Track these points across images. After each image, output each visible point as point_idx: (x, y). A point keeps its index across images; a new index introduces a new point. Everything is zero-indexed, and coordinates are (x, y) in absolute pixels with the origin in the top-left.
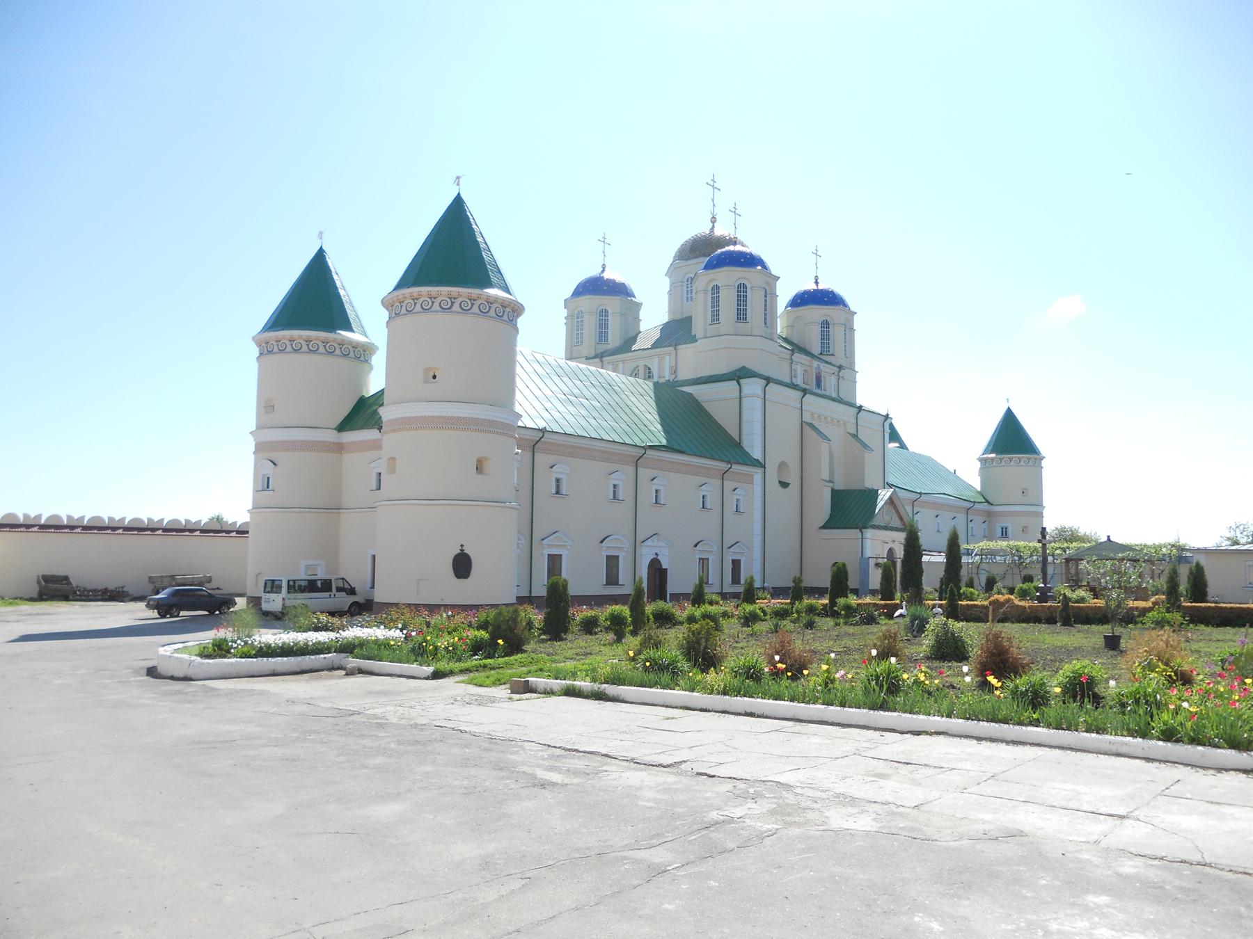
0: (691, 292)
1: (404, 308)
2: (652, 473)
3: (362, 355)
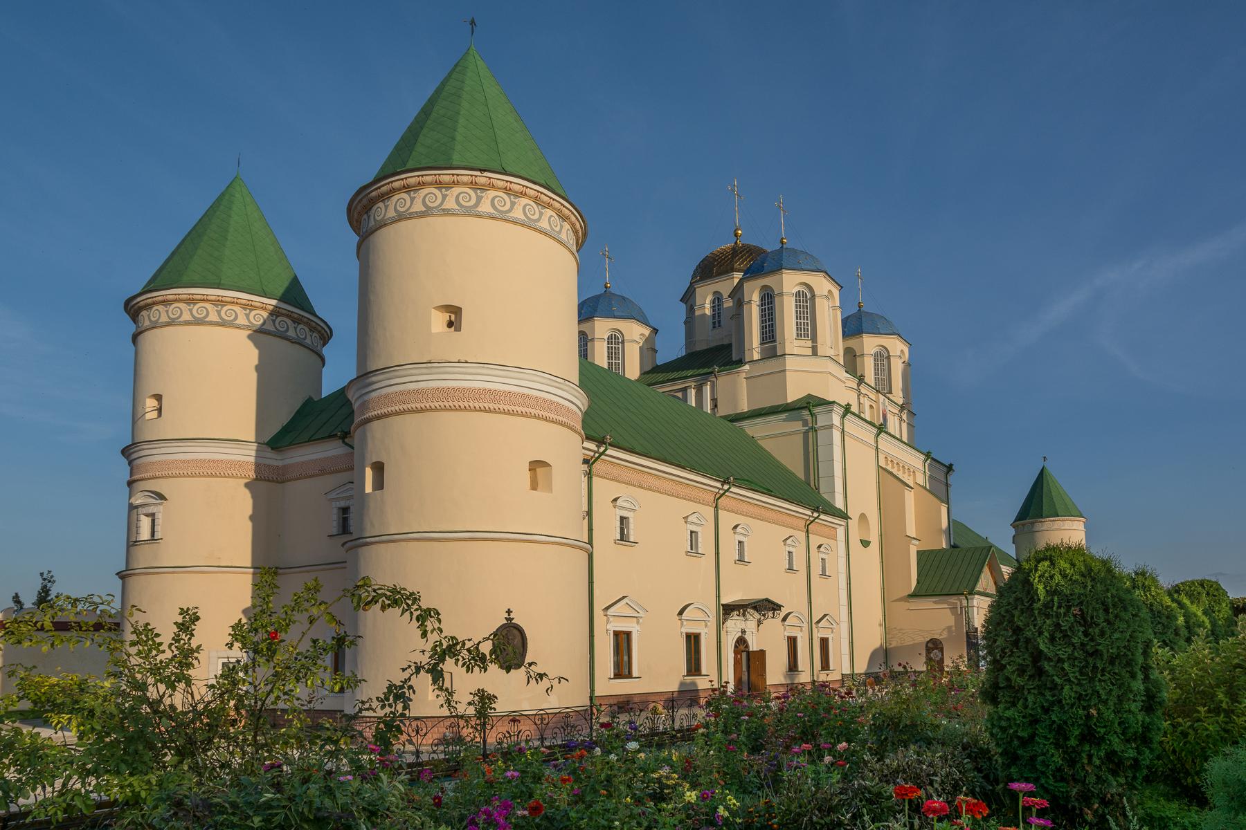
0: (719, 316)
1: (391, 208)
2: (737, 519)
3: (308, 337)
